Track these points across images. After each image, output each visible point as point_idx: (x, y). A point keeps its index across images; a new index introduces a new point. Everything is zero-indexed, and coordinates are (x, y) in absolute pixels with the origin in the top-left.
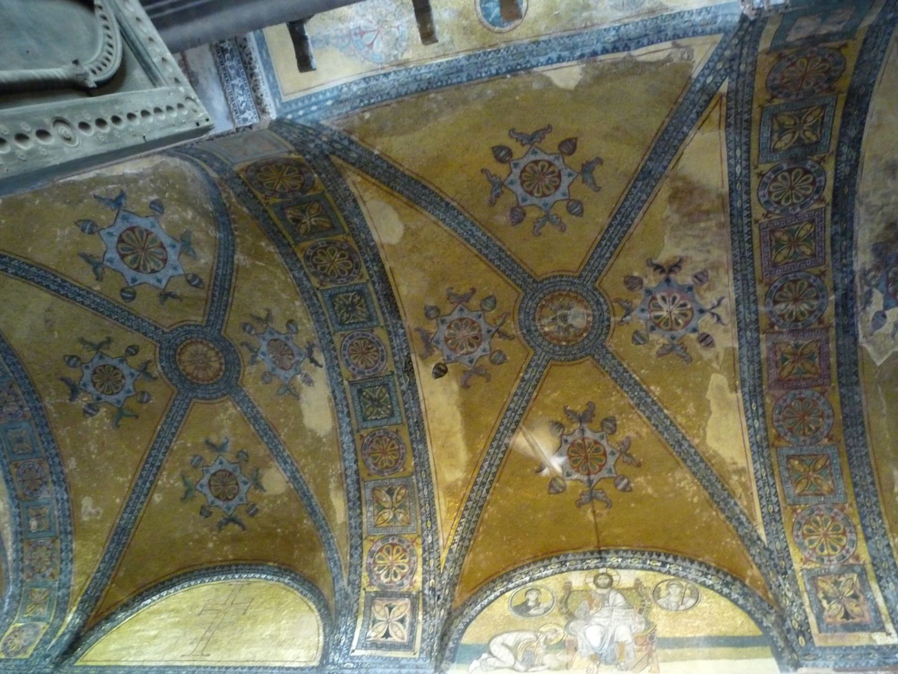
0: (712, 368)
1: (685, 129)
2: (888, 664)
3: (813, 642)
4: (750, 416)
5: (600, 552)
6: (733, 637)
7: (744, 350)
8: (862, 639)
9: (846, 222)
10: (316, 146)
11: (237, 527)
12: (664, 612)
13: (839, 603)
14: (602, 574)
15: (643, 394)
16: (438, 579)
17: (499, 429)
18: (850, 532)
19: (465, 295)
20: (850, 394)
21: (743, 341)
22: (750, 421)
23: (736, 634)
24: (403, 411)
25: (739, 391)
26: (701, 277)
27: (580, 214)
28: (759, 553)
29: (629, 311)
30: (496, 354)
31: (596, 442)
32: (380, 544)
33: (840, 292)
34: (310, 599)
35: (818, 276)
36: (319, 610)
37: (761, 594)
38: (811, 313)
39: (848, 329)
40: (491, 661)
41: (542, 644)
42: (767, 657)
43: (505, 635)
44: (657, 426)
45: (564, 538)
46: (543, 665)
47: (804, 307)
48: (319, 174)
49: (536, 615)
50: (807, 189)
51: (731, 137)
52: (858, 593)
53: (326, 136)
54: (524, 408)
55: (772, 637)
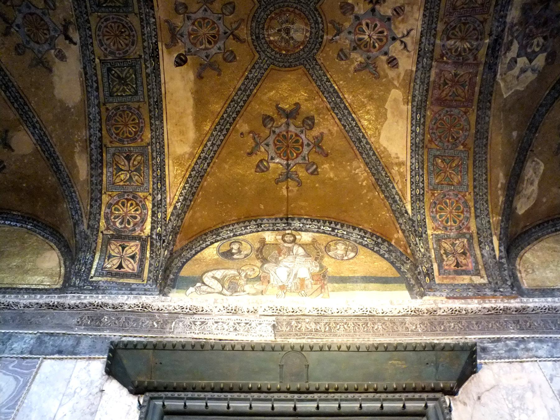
0: (393, 84)
2: (480, 295)
3: (434, 281)
4: (414, 123)
6: (381, 277)
8: (466, 279)
12: (333, 260)
13: (454, 257)
14: (288, 234)
15: (338, 100)
16: (164, 228)
17: (223, 116)
18: (467, 211)
20: (483, 116)
22: (414, 127)
24: (145, 91)
25: (410, 104)
26: (398, 11)
28: (405, 222)
30: (228, 53)
31: (297, 135)
33: (494, 37)
34: (52, 241)
35: (482, 22)
36: (60, 249)
37: (401, 250)
39: (491, 67)
40: (203, 288)
42: (404, 290)
43: (214, 272)
44: (345, 126)
45: (262, 207)
46: (244, 291)
47: (467, 45)
49: (238, 259)
52: (466, 251)
54: (245, 102)
55: (407, 278)
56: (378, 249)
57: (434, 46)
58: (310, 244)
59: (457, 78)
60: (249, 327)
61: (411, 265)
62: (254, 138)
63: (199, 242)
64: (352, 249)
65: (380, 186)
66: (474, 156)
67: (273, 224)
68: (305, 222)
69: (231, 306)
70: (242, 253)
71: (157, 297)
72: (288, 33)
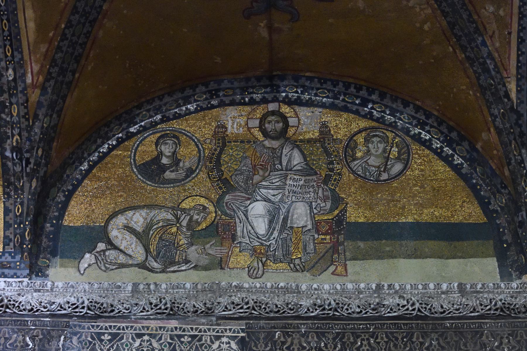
5: (271, 78)
14: (273, 113)
16: (25, 134)
23: (452, 220)
40: (112, 254)
41: (185, 230)
43: (130, 213)
46: (187, 262)
55: (499, 226)
56: (451, 152)
58: (315, 141)
60: (198, 343)
61: (509, 199)
63: (95, 141)
64: (399, 152)
68: (307, 84)
69: (164, 301)
70: (181, 164)
71: (26, 280)
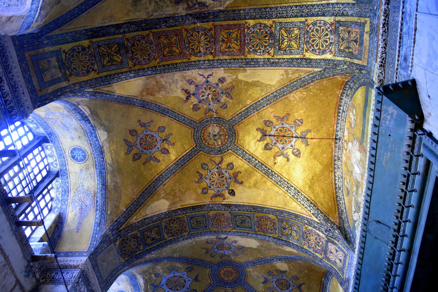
1: (116, 97)
5: (336, 139)
7: (224, 66)
9: (160, 22)
10: (112, 236)
11: (303, 286)
15: (251, 107)
16: (323, 226)
19: (199, 175)
21: (219, 66)
25: (245, 68)
26: (191, 82)
27: (164, 128)
29: (210, 110)
31: (277, 130)
32: (306, 242)
35: (188, 32)
38: (206, 34)
45: (325, 155)
48: (129, 233)
50: (142, 43)
51: (116, 81)
52: (348, 30)
53: (109, 232)
54: (256, 160)
57: (205, 60)
59: (225, 39)
62: (279, 156)
63: (340, 203)
65: (305, 85)
66: (279, 18)
67: (339, 149)
68: (339, 128)
72: (215, 135)
